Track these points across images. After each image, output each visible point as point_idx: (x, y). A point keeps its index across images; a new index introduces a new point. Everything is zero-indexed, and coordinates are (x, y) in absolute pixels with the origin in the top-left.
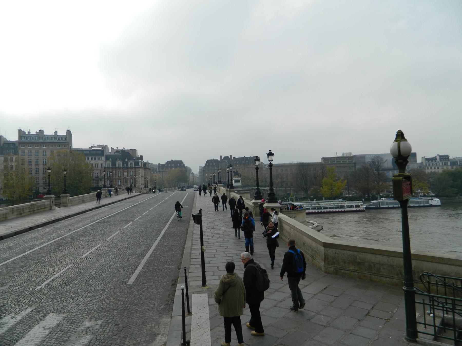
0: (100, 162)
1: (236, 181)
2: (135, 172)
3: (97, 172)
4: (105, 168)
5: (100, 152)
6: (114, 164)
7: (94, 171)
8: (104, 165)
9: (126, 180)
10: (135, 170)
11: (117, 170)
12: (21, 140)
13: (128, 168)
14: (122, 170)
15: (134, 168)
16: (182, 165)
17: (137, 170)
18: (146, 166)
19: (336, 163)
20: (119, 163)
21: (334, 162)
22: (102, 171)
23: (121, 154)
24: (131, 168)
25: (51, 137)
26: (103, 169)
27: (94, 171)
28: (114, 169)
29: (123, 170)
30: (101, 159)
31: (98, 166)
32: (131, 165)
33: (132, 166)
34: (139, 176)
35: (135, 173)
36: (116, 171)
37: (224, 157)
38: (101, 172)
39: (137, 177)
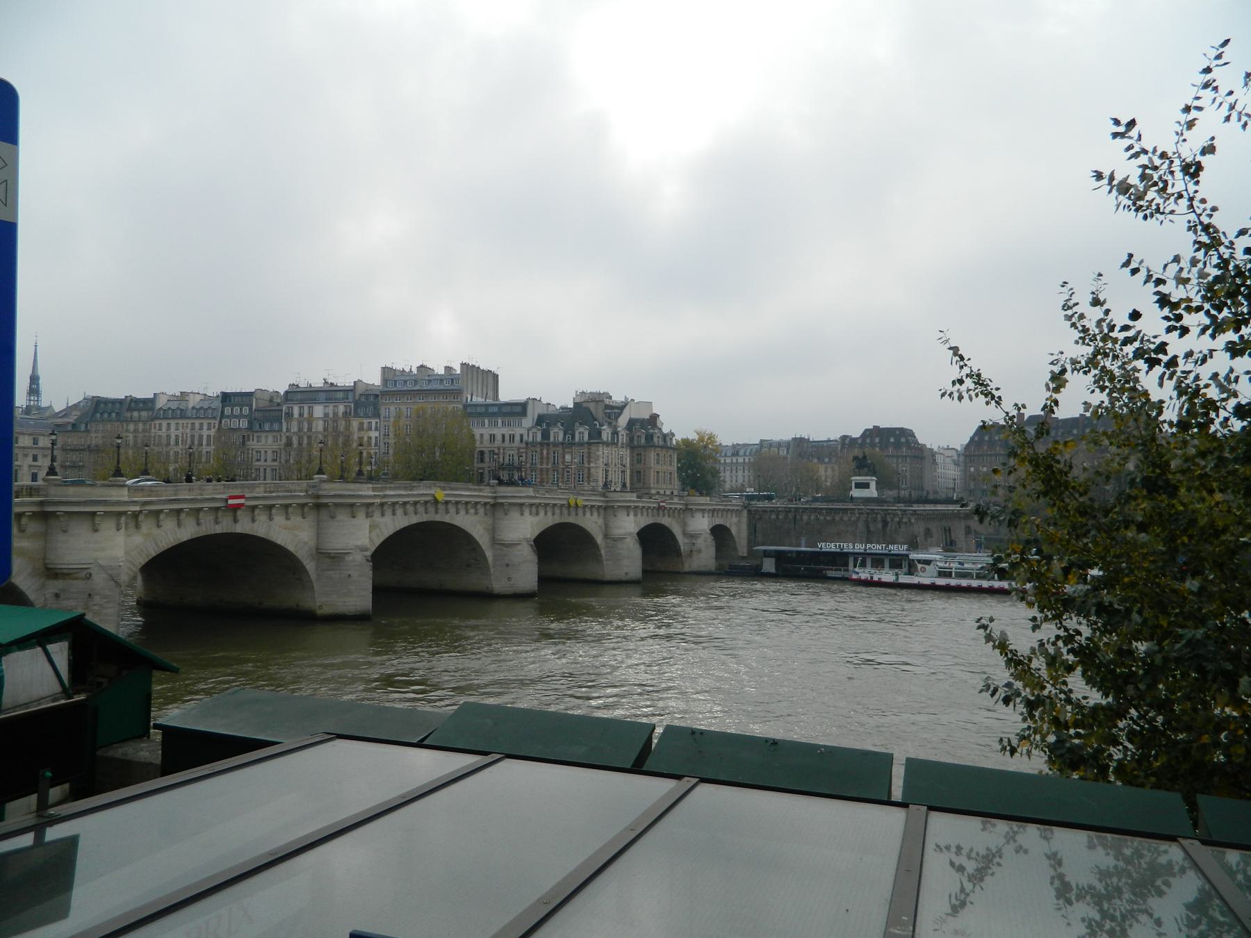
0: (518, 431)
1: (859, 486)
3: (511, 452)
4: (527, 443)
5: (519, 409)
6: (546, 435)
8: (525, 438)
9: (568, 472)
10: (589, 449)
11: (552, 449)
12: (387, 387)
13: (572, 444)
16: (903, 440)
17: (593, 448)
18: (652, 439)
20: (557, 434)
24: (581, 444)
25: (441, 379)
26: (523, 445)
29: (563, 450)
30: (520, 425)
35: (589, 457)
36: (548, 450)
37: (1030, 417)
39: (592, 465)
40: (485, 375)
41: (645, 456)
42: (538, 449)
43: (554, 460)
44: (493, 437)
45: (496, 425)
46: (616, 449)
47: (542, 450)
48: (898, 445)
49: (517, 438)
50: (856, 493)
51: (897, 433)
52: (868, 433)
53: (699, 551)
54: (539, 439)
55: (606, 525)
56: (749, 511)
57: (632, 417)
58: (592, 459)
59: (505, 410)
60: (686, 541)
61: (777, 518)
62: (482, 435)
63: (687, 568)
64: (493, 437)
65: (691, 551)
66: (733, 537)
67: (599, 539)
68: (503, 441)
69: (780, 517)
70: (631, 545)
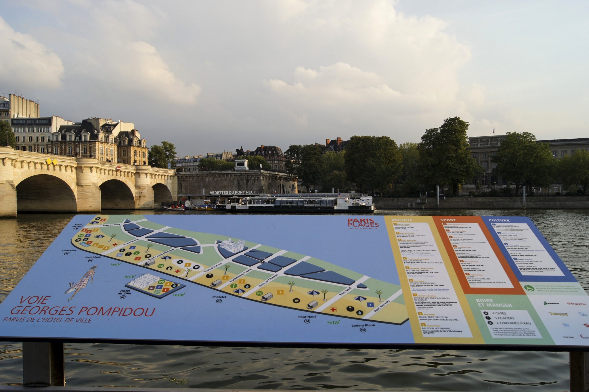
2: (90, 148)
4: (52, 142)
5: (47, 122)
6: (64, 137)
7: (39, 146)
13: (80, 142)
14: (73, 145)
15: (88, 143)
19: (489, 146)
21: (487, 144)
22: (49, 146)
23: (80, 125)
24: (85, 142)
27: (39, 146)
28: (63, 143)
29: (74, 145)
31: (45, 139)
32: (84, 138)
33: (86, 140)
34: (94, 153)
36: (65, 146)
37: (332, 141)
38: (47, 148)
40: (28, 102)
41: (127, 151)
42: (59, 145)
43: (69, 151)
44: (31, 138)
45: (33, 131)
46: (108, 146)
47: (61, 146)
48: (273, 155)
49: (46, 139)
50: (237, 168)
51: (273, 149)
52: (259, 149)
53: (144, 196)
54: (60, 139)
55: (78, 179)
56: (178, 177)
57: (122, 130)
58: (92, 151)
59: (37, 122)
60: (137, 191)
61: (193, 180)
62: (24, 137)
63: (137, 207)
64: (31, 138)
65: (140, 197)
66: (169, 191)
67: (73, 187)
68: (37, 140)
69: (195, 179)
70: (94, 190)
